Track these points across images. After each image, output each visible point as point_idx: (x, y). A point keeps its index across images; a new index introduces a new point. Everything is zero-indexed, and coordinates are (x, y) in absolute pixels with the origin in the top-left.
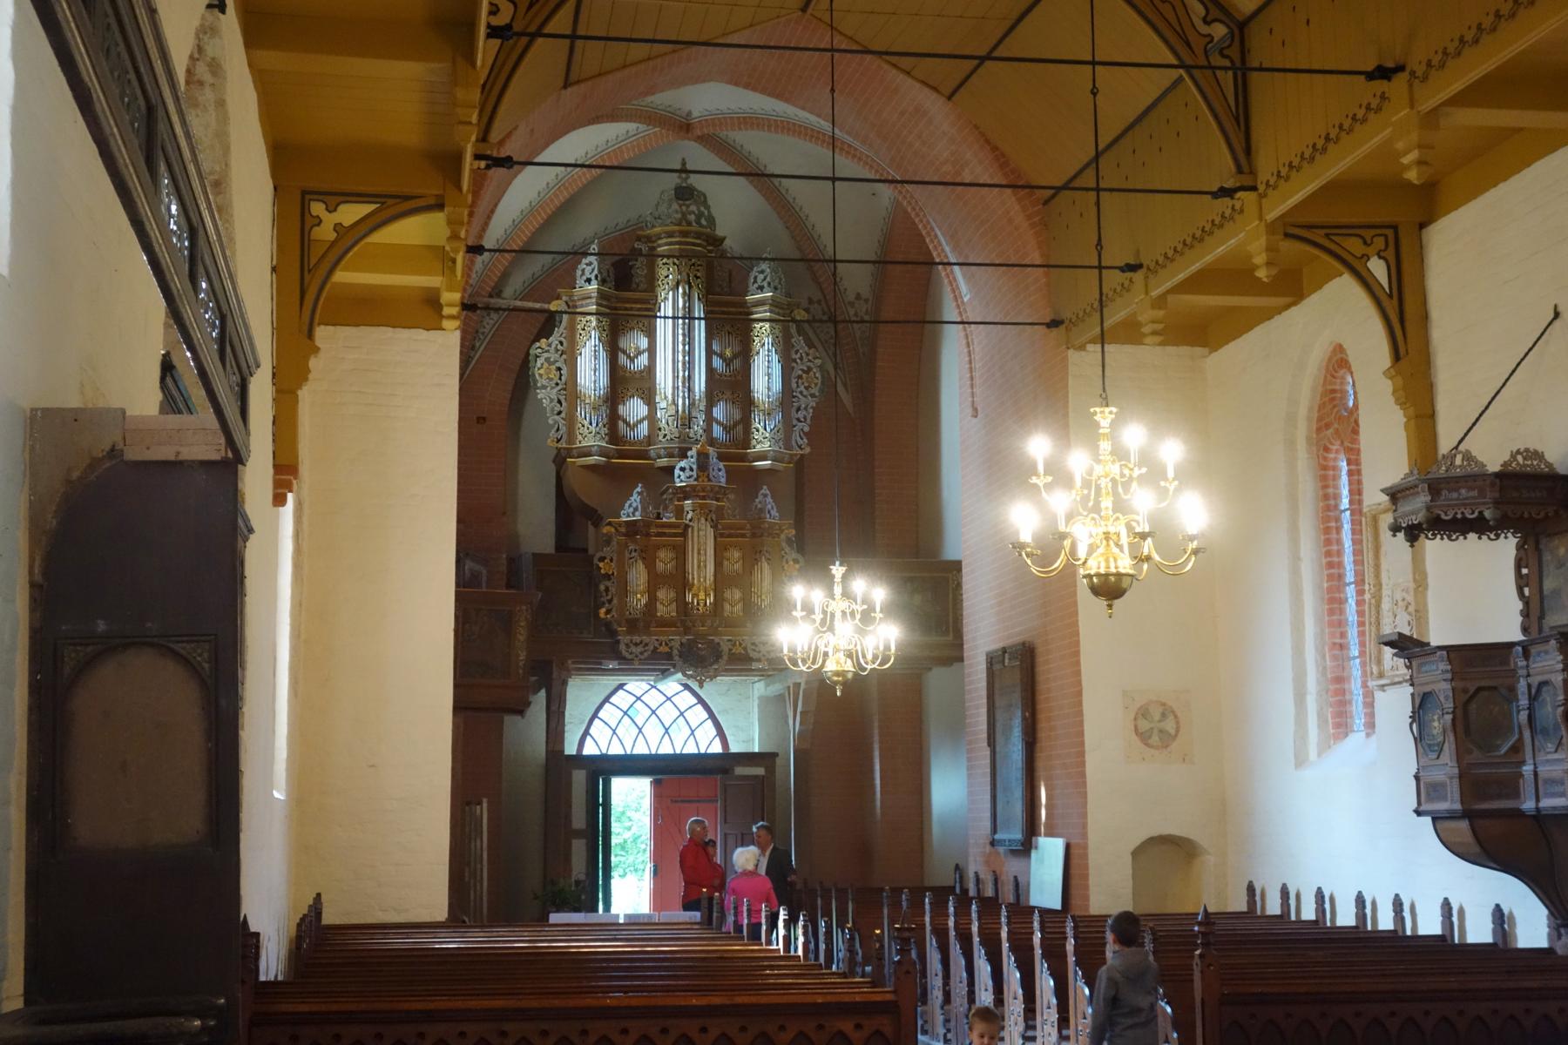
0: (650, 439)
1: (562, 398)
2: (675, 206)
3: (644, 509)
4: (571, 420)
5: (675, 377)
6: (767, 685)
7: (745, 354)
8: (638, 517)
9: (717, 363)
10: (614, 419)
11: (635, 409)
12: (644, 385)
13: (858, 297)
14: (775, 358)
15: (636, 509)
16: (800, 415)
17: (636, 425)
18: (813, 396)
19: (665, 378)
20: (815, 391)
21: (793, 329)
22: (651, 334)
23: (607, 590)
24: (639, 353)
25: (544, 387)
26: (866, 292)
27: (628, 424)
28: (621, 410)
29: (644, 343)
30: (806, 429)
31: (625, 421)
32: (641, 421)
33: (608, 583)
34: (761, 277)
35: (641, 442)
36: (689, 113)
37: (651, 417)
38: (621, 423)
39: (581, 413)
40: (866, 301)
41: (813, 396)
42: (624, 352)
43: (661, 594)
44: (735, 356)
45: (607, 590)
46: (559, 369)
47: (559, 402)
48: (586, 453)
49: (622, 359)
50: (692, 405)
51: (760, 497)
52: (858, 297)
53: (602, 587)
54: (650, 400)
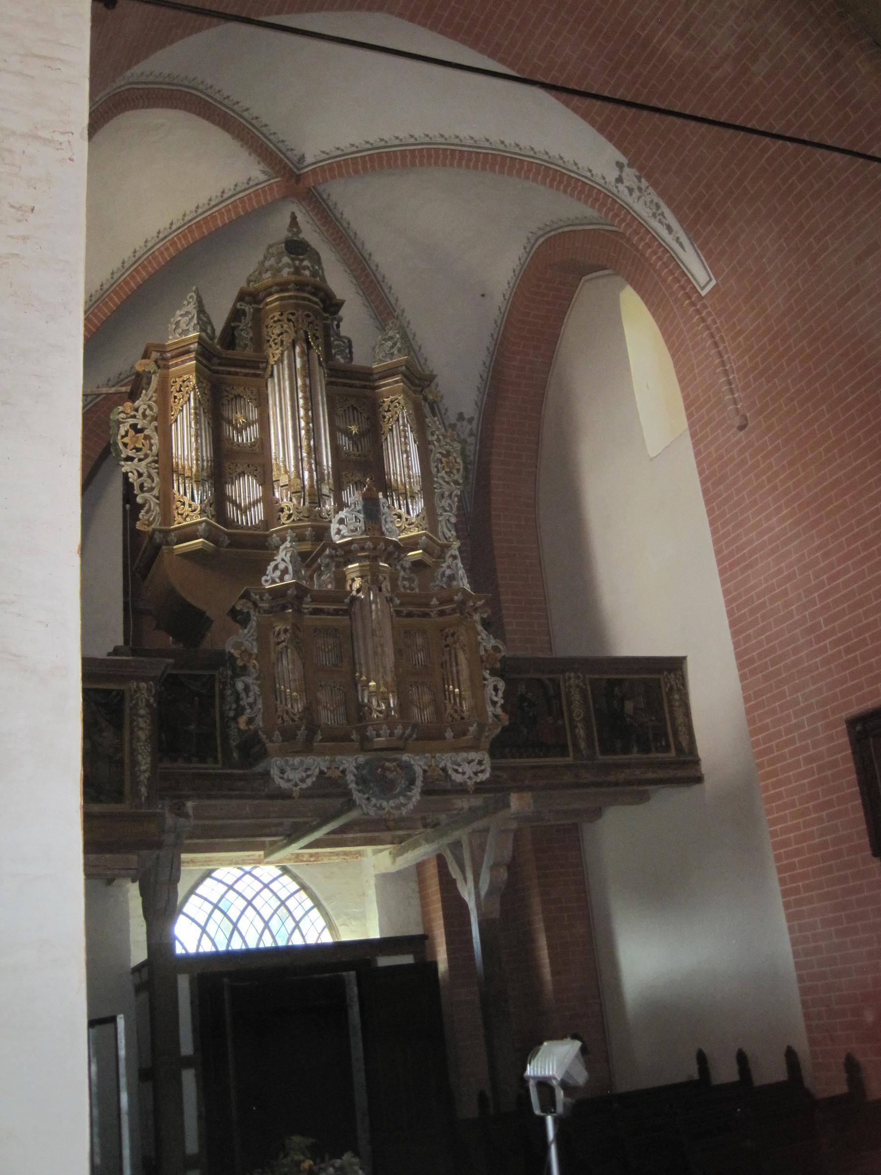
0: (266, 524)
1: (154, 472)
2: (286, 260)
3: (296, 573)
4: (166, 499)
5: (298, 448)
6: (395, 856)
7: (373, 435)
8: (289, 579)
9: (344, 441)
10: (219, 502)
11: (245, 489)
12: (258, 461)
13: (461, 417)
14: (411, 436)
15: (285, 571)
16: (445, 503)
17: (248, 507)
18: (456, 483)
19: (283, 450)
20: (458, 477)
21: (427, 410)
22: (262, 403)
23: (247, 689)
24: (248, 424)
25: (130, 459)
26: (470, 409)
27: (238, 507)
28: (229, 490)
29: (254, 414)
30: (453, 520)
31: (234, 503)
32: (255, 503)
33: (249, 680)
34: (390, 343)
35: (256, 527)
36: (302, 158)
37: (268, 500)
38: (230, 507)
39: (178, 489)
40: (470, 421)
41: (456, 483)
42: (230, 422)
43: (323, 696)
44: (361, 434)
45: (247, 689)
46: (147, 438)
47: (150, 476)
48: (188, 534)
49: (229, 431)
50: (321, 479)
51: (449, 561)
52: (461, 417)
53: (240, 686)
54: (266, 480)
